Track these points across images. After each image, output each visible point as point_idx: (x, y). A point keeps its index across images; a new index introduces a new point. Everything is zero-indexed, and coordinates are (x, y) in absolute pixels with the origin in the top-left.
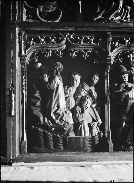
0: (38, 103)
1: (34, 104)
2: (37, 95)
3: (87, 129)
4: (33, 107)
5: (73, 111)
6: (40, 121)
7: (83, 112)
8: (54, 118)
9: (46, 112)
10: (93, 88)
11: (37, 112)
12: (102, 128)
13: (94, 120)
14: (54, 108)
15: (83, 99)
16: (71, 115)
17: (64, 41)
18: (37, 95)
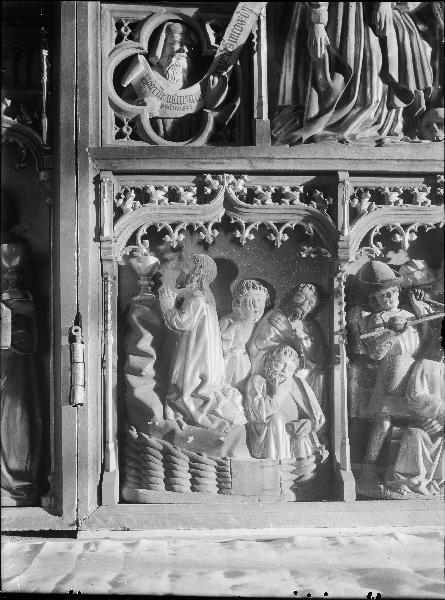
0: (149, 368)
1: (138, 372)
2: (146, 342)
3: (285, 438)
4: (131, 379)
5: (242, 387)
6: (150, 414)
7: (270, 391)
8: (192, 408)
9: (166, 388)
10: (298, 326)
11: (144, 388)
12: (327, 435)
13: (302, 415)
14: (191, 382)
15: (272, 354)
16: (239, 398)
17: (220, 198)
18: (146, 342)
